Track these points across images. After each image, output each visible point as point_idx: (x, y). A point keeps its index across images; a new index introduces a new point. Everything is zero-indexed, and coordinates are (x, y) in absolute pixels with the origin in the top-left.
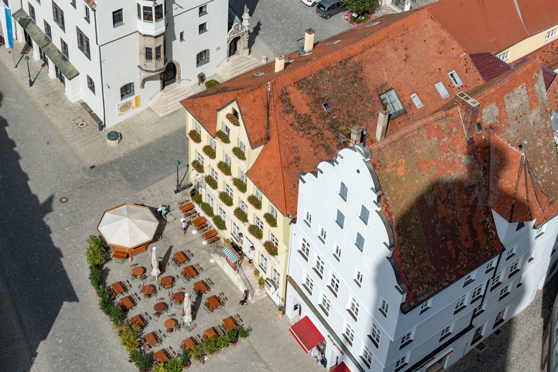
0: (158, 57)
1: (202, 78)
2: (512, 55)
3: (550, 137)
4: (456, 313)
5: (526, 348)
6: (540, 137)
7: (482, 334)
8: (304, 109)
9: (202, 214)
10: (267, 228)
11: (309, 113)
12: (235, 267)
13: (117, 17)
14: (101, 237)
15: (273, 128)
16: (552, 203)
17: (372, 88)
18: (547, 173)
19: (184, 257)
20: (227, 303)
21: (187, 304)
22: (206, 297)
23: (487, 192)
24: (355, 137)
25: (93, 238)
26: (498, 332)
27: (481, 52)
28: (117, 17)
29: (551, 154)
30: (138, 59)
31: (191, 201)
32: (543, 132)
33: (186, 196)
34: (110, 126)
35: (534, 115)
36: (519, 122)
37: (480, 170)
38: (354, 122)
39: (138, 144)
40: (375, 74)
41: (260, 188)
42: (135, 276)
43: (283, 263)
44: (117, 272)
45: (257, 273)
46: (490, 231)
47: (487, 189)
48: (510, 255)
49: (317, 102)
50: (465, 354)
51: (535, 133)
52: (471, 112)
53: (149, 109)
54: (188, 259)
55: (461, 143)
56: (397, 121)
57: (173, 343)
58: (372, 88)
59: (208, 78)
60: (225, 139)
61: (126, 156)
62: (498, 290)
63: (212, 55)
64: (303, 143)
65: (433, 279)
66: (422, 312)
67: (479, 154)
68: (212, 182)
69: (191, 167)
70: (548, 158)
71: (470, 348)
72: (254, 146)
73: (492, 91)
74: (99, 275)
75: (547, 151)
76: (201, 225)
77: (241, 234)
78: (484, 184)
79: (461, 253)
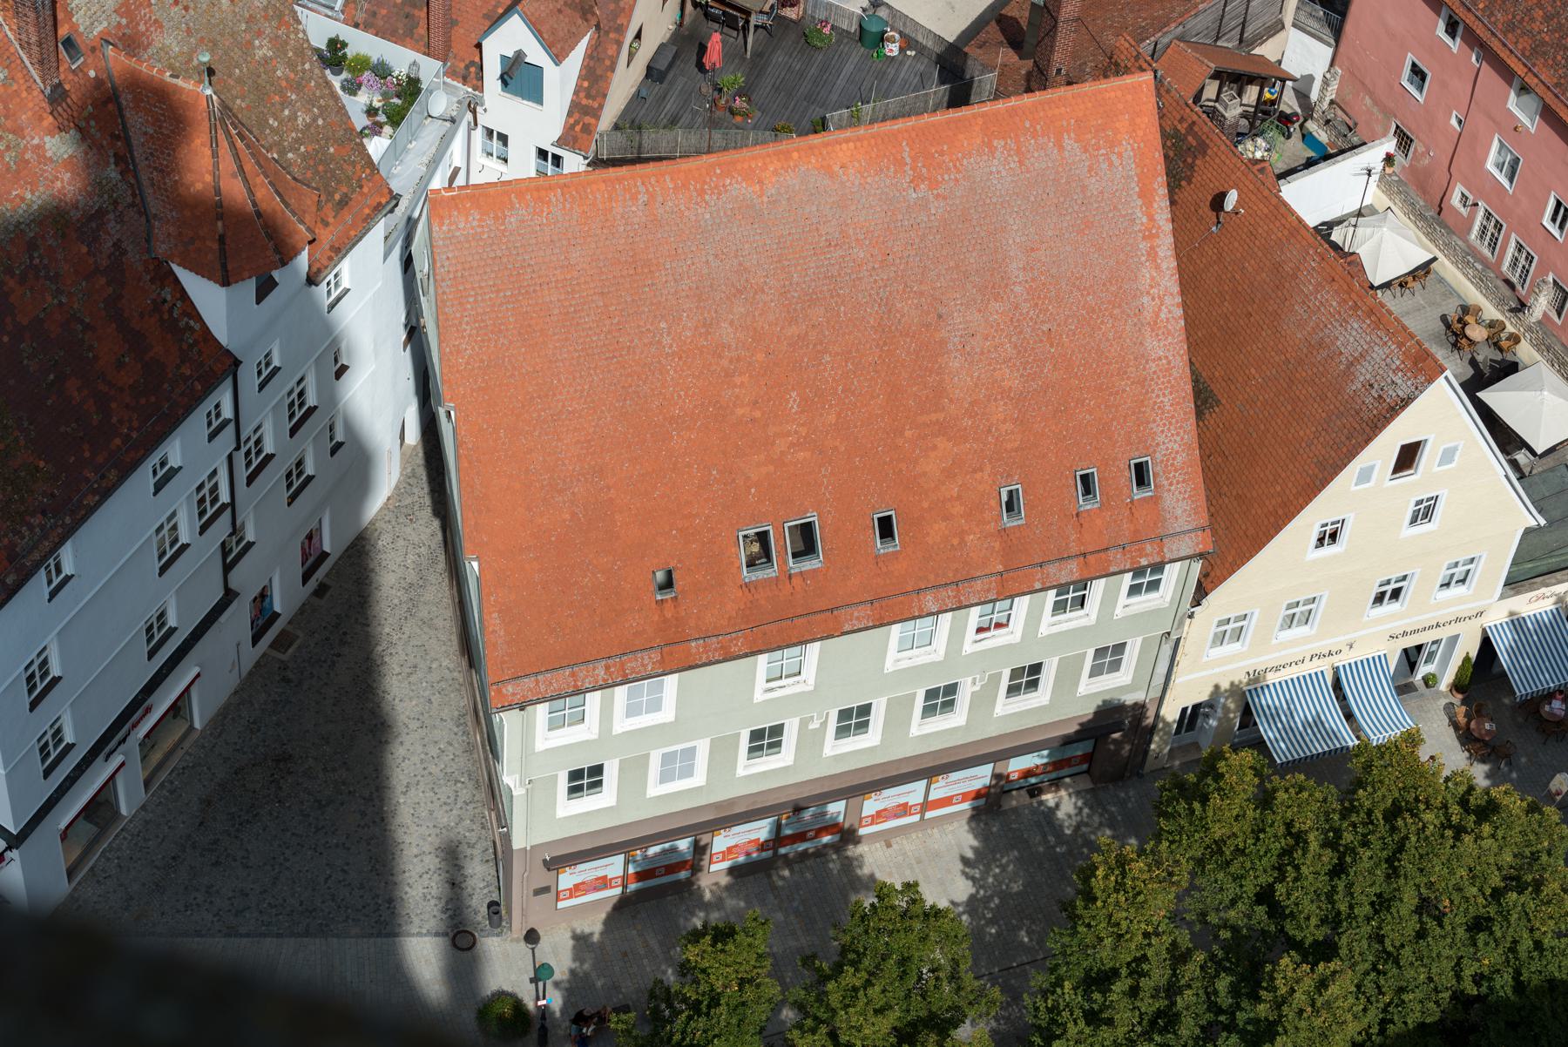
3: (288, 25)
4: (163, 570)
5: (409, 610)
6: (259, 34)
7: (277, 608)
16: (344, 203)
18: (308, 126)
23: (143, 219)
26: (321, 590)
29: (304, 71)
32: (266, 17)
36: (186, 8)
37: (108, 164)
46: (182, 324)
47: (143, 211)
48: (265, 374)
50: (244, 674)
51: (243, 27)
52: (32, 15)
55: (31, 105)
62: (273, 476)
65: (53, 495)
66: (53, 595)
67: (93, 123)
70: (299, 84)
71: (251, 655)
75: (291, 65)
78: (129, 200)
79: (114, 405)
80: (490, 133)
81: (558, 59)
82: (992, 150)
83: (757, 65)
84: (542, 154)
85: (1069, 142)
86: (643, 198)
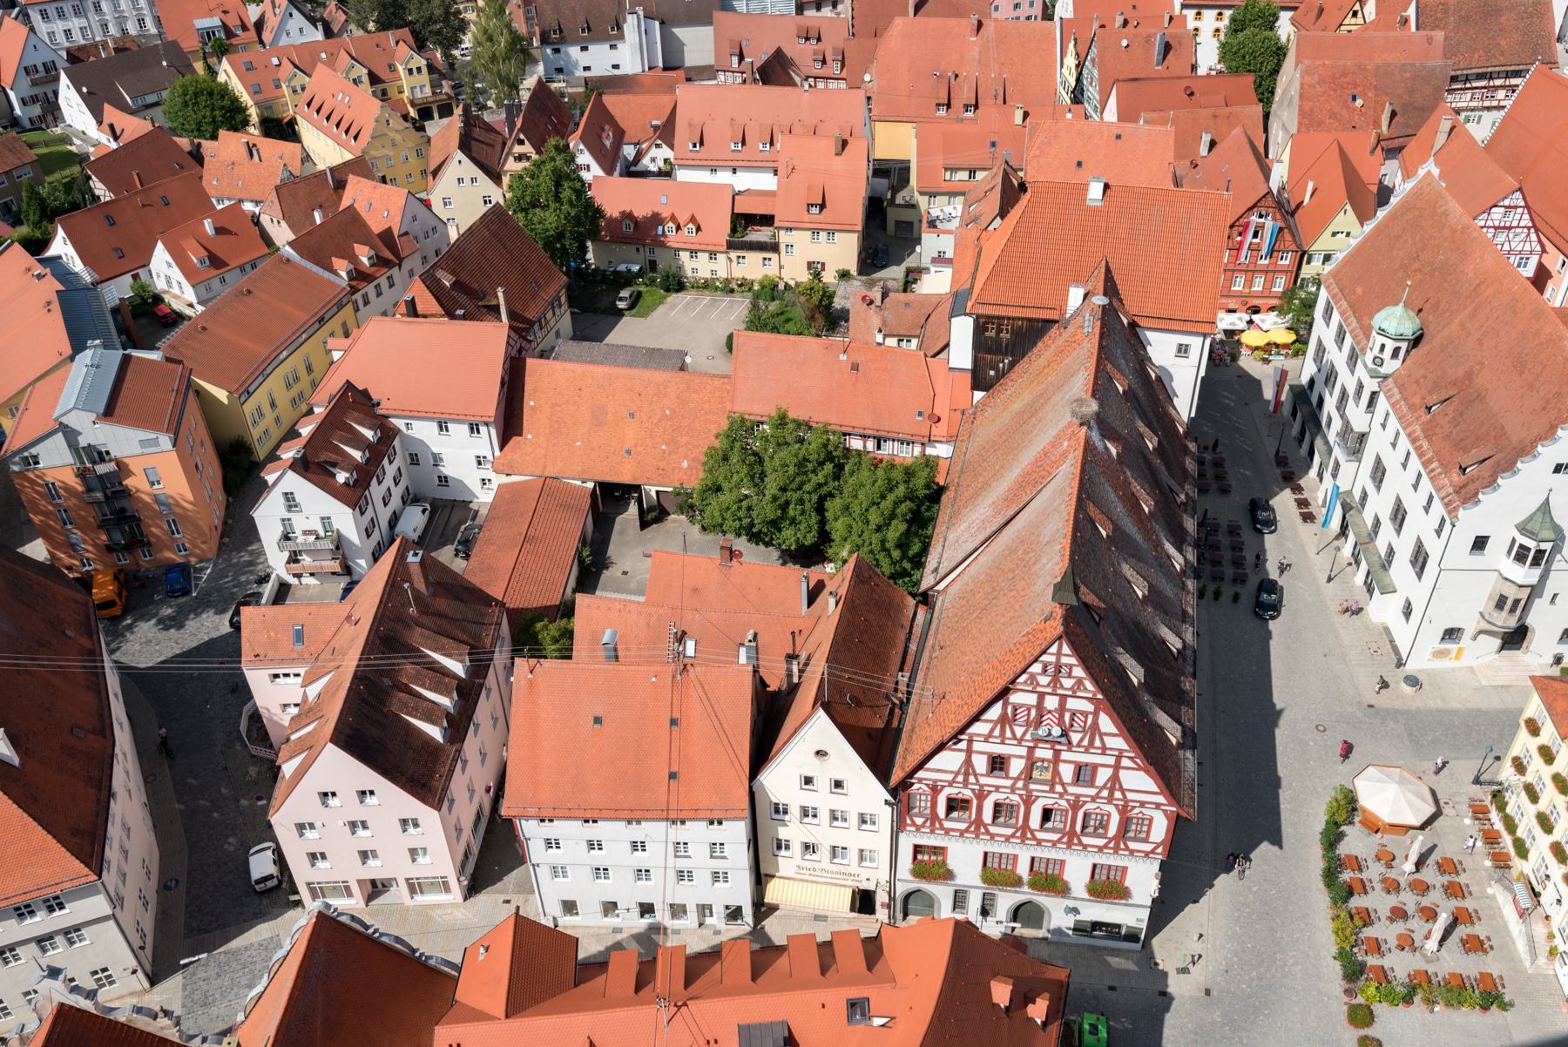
9: (1499, 826)
12: (1523, 914)
20: (1491, 953)
21: (1438, 928)
22: (1462, 931)
25: (1342, 788)
33: (1484, 795)
34: (1411, 667)
39: (1440, 704)
42: (1378, 858)
44: (1355, 842)
45: (1551, 936)
53: (1471, 669)
54: (1457, 873)
57: (1400, 965)
68: (1532, 794)
74: (1332, 837)
76: (1491, 838)
77: (1548, 877)
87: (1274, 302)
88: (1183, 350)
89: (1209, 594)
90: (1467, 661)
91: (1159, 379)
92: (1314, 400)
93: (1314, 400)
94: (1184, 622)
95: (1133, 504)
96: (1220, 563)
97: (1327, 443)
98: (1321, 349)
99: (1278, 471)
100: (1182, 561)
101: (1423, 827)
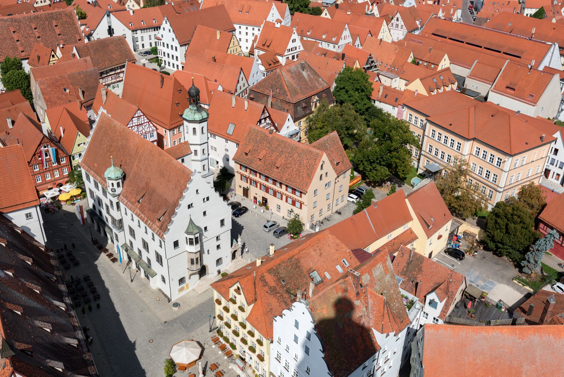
0: (197, 263)
1: (219, 272)
2: (371, 249)
8: (273, 284)
9: (224, 342)
10: (258, 347)
11: (276, 285)
12: (242, 369)
13: (176, 244)
14: (171, 359)
15: (258, 295)
16: (402, 322)
17: (305, 271)
19: (215, 366)
24: (299, 296)
25: (167, 360)
27: (356, 248)
28: (176, 244)
30: (186, 264)
31: (217, 336)
35: (388, 278)
38: (298, 288)
39: (189, 308)
40: (306, 263)
41: (253, 326)
43: (267, 366)
45: (254, 372)
49: (279, 279)
53: (194, 290)
54: (218, 368)
56: (319, 286)
58: (305, 271)
59: (222, 273)
60: (234, 302)
61: (183, 315)
63: (224, 260)
64: (274, 302)
69: (217, 318)
72: (249, 304)
73: (366, 267)
80: (424, 313)
81: (441, 302)
82: (535, 335)
83: (476, 308)
84: (434, 319)
85: (551, 336)
86: (465, 332)
87: (67, 179)
88: (29, 216)
89: (87, 310)
90: (190, 288)
91: (23, 232)
92: (98, 213)
93: (98, 213)
94: (75, 331)
95: (31, 293)
96: (86, 295)
97: (109, 228)
98: (92, 193)
99: (95, 247)
100: (64, 305)
101: (200, 358)
